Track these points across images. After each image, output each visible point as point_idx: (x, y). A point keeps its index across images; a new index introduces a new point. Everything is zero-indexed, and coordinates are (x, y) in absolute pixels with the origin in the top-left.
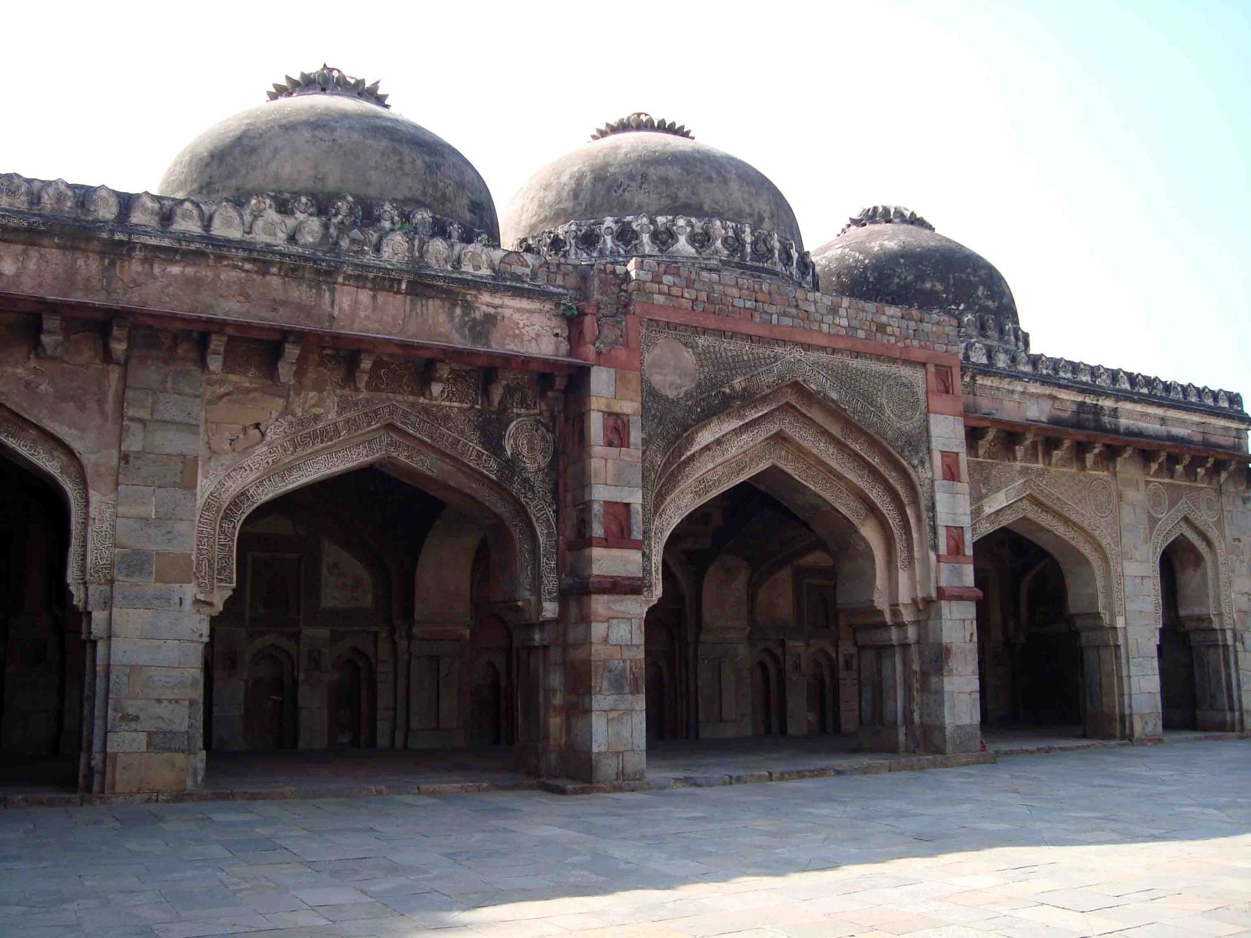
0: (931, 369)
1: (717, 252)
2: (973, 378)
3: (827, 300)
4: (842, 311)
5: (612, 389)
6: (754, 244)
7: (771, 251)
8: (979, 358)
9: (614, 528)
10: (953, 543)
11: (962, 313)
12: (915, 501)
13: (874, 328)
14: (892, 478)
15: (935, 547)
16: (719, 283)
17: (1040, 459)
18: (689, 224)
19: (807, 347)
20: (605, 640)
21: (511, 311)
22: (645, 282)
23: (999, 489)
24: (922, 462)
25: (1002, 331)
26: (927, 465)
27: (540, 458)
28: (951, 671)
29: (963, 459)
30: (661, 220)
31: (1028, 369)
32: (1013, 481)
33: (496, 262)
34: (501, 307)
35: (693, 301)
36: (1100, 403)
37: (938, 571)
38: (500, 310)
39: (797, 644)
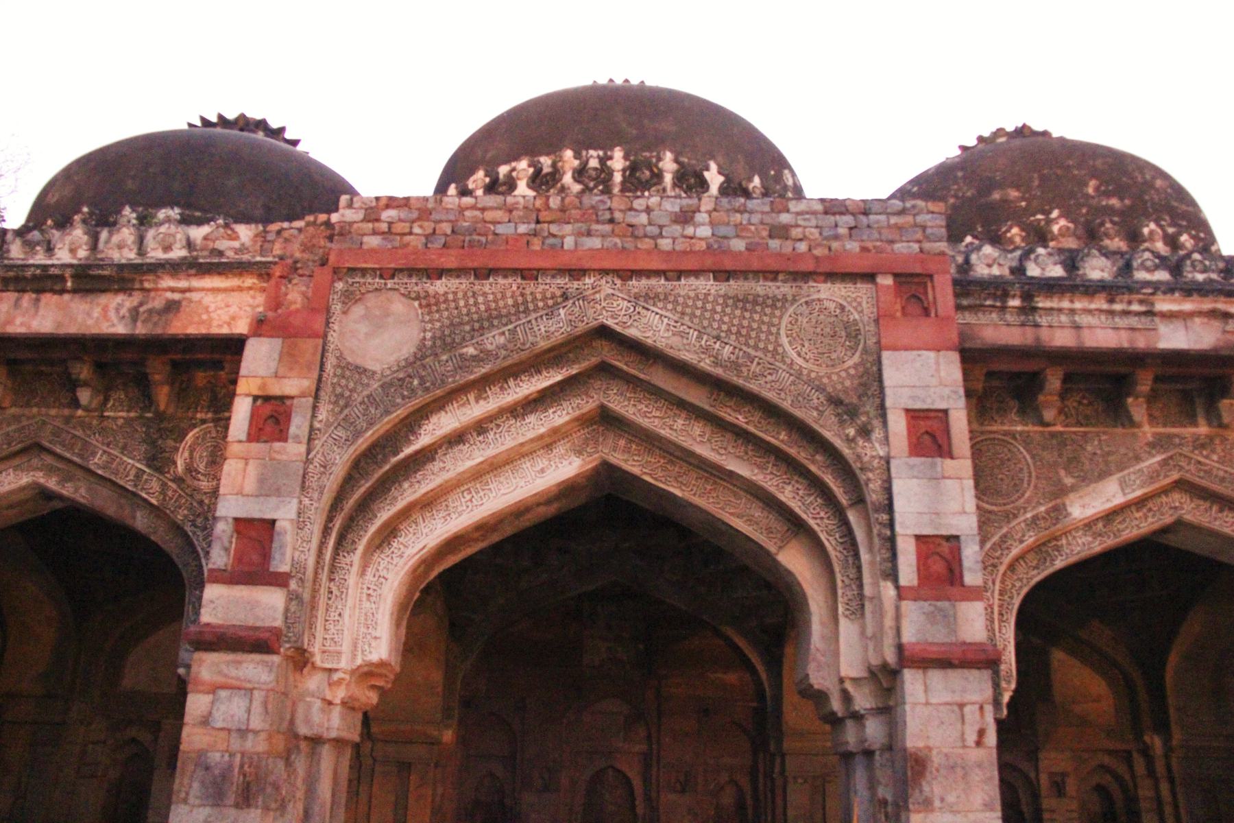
0: (886, 281)
2: (1027, 297)
4: (702, 217)
5: (273, 365)
6: (632, 170)
7: (658, 176)
9: (255, 558)
10: (938, 567)
11: (1055, 221)
12: (859, 500)
13: (765, 233)
14: (817, 466)
15: (893, 575)
16: (474, 207)
17: (1201, 420)
19: (626, 274)
20: (205, 721)
21: (201, 294)
22: (351, 224)
23: (1103, 475)
24: (865, 432)
26: (877, 434)
31: (1163, 276)
32: (1138, 459)
33: (199, 242)
34: (189, 290)
35: (427, 236)
37: (898, 617)
38: (188, 295)
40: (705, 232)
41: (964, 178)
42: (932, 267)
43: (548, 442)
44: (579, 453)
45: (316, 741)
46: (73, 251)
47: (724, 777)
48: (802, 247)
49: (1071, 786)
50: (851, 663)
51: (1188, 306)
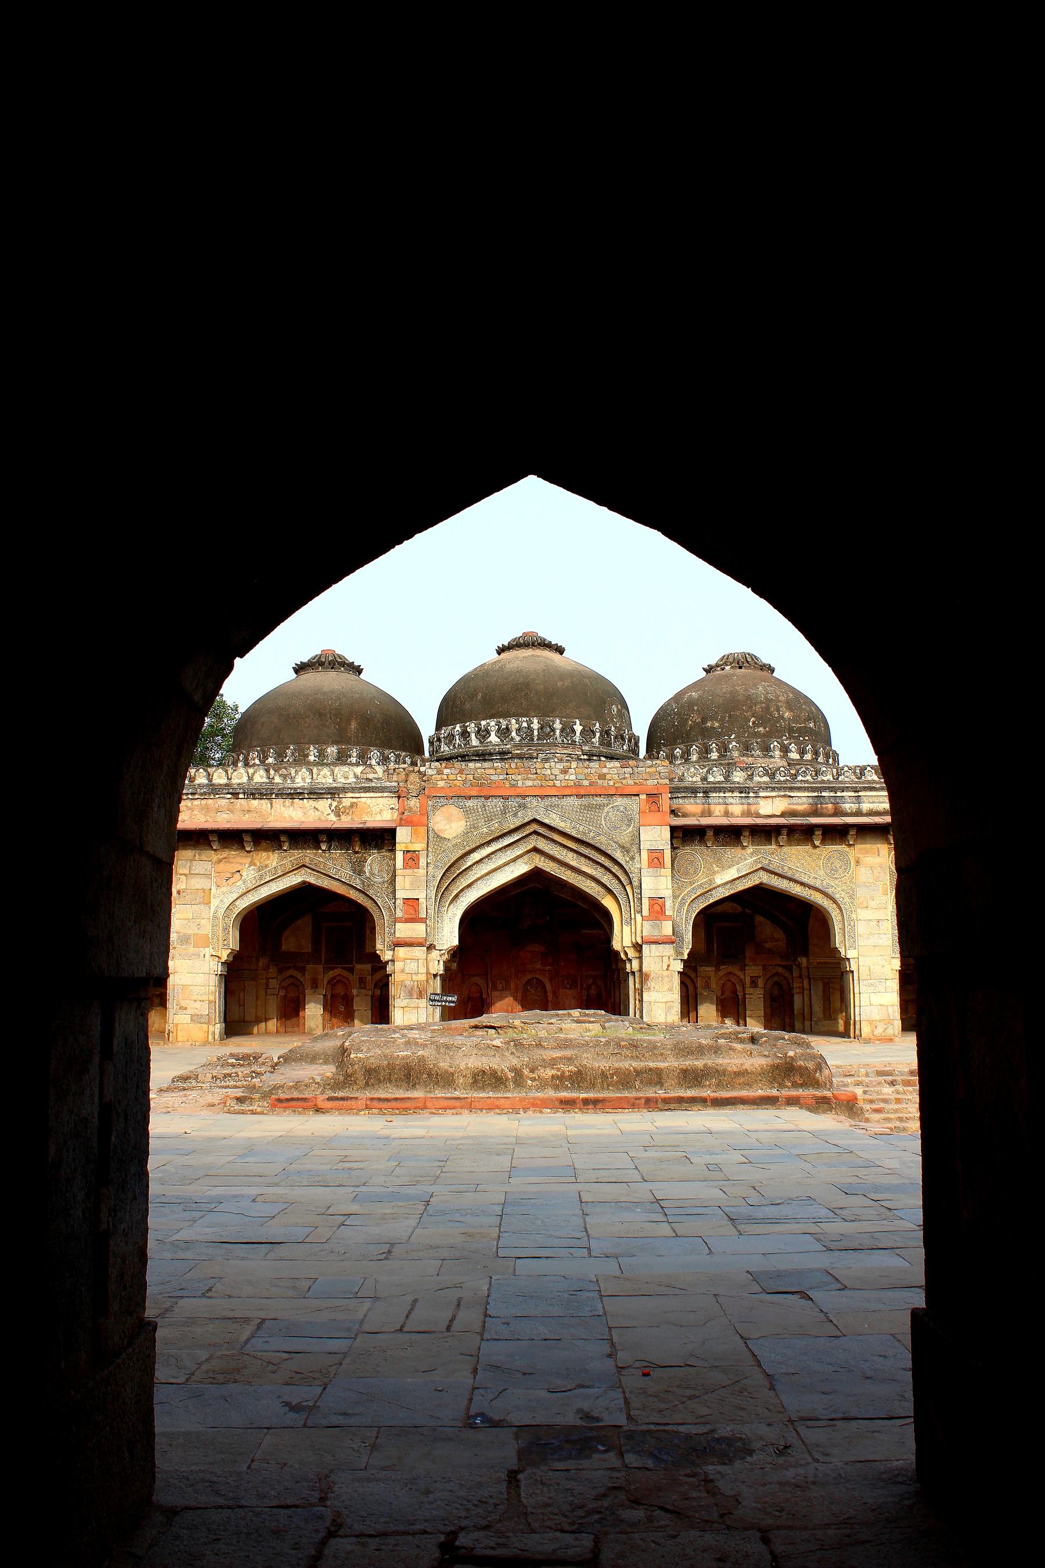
0: (643, 797)
1: (512, 739)
3: (560, 766)
4: (572, 771)
7: (553, 730)
8: (717, 776)
9: (412, 912)
10: (657, 908)
11: (730, 742)
18: (498, 724)
19: (542, 797)
20: (403, 971)
24: (632, 858)
25: (766, 750)
26: (637, 858)
27: (385, 875)
28: (649, 989)
29: (668, 854)
30: (483, 723)
31: (766, 779)
32: (745, 859)
36: (839, 794)
39: (709, 969)
40: (573, 777)
41: (698, 710)
42: (661, 791)
43: (514, 860)
44: (526, 863)
45: (435, 976)
46: (303, 779)
47: (591, 981)
48: (611, 783)
49: (761, 983)
50: (627, 942)
51: (773, 794)
